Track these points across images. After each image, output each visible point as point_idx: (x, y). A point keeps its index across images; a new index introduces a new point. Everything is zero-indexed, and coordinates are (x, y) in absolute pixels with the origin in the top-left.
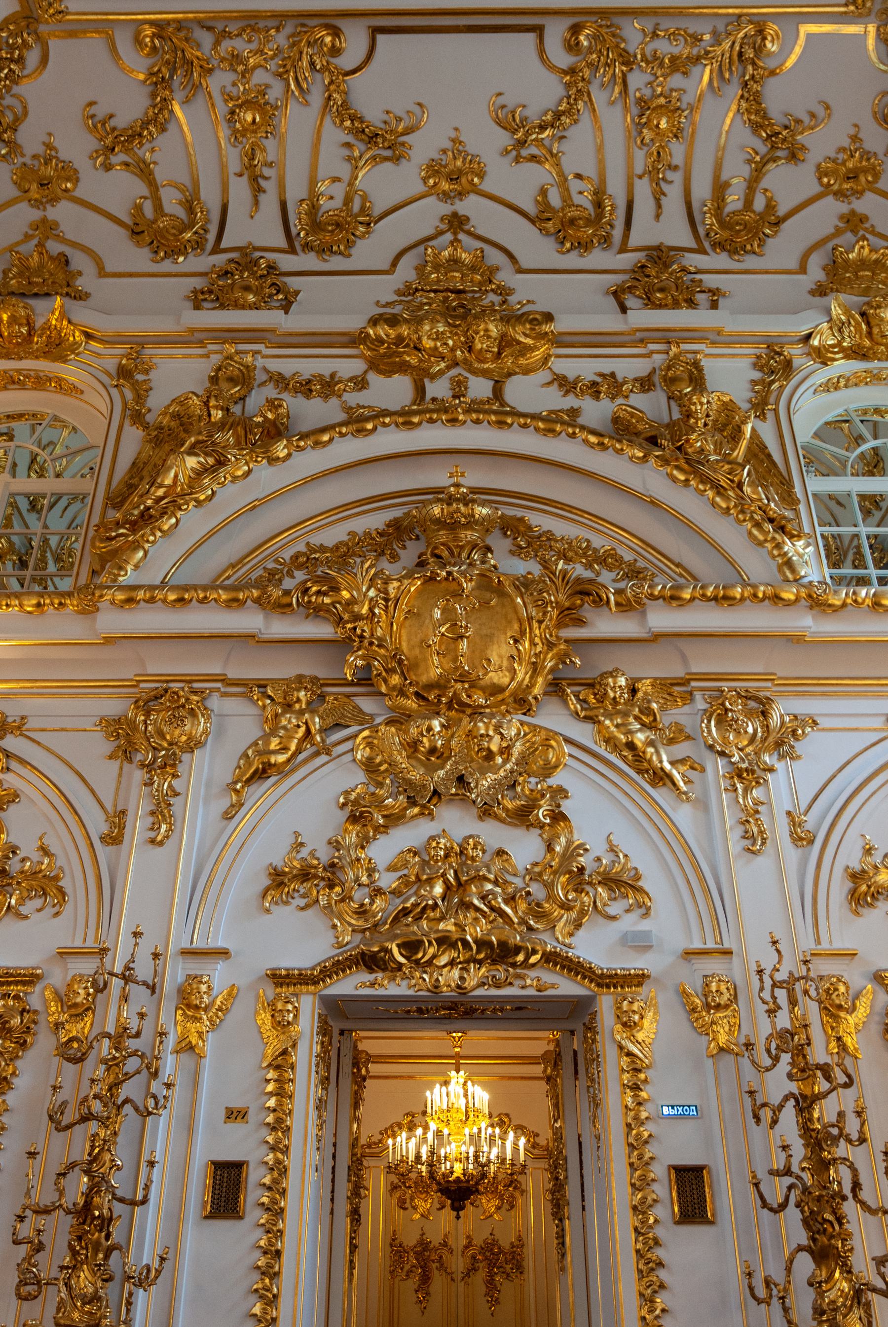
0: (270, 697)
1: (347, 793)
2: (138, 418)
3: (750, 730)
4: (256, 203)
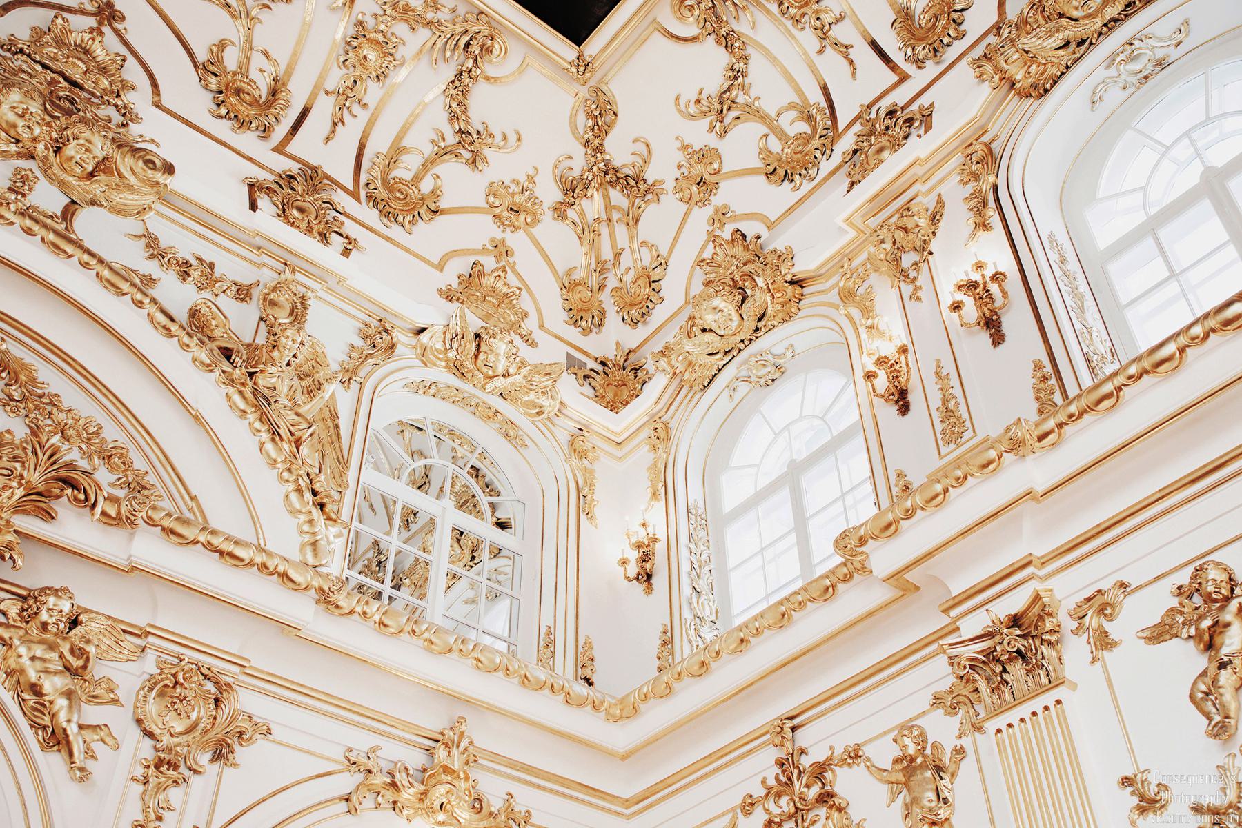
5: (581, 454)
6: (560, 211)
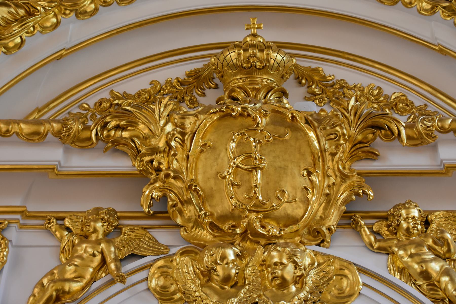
0: (68, 229)
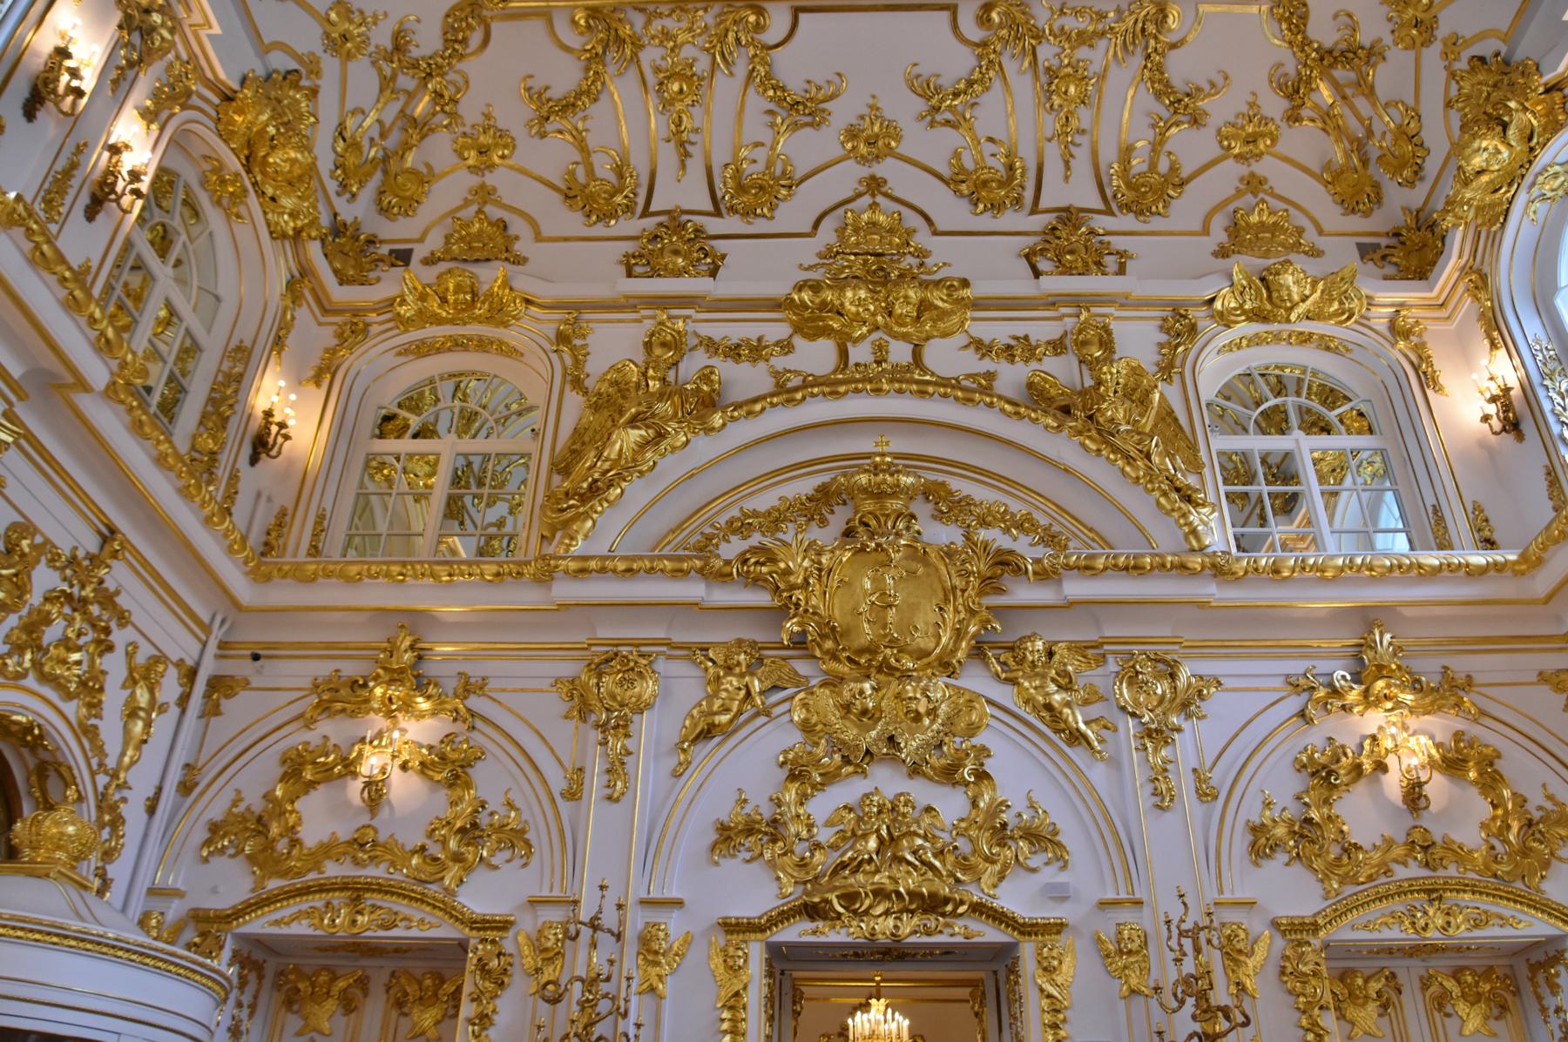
0: (711, 660)
1: (785, 752)
2: (577, 384)
3: (1159, 691)
4: (683, 166)
5: (1406, 334)
6: (1293, 117)
